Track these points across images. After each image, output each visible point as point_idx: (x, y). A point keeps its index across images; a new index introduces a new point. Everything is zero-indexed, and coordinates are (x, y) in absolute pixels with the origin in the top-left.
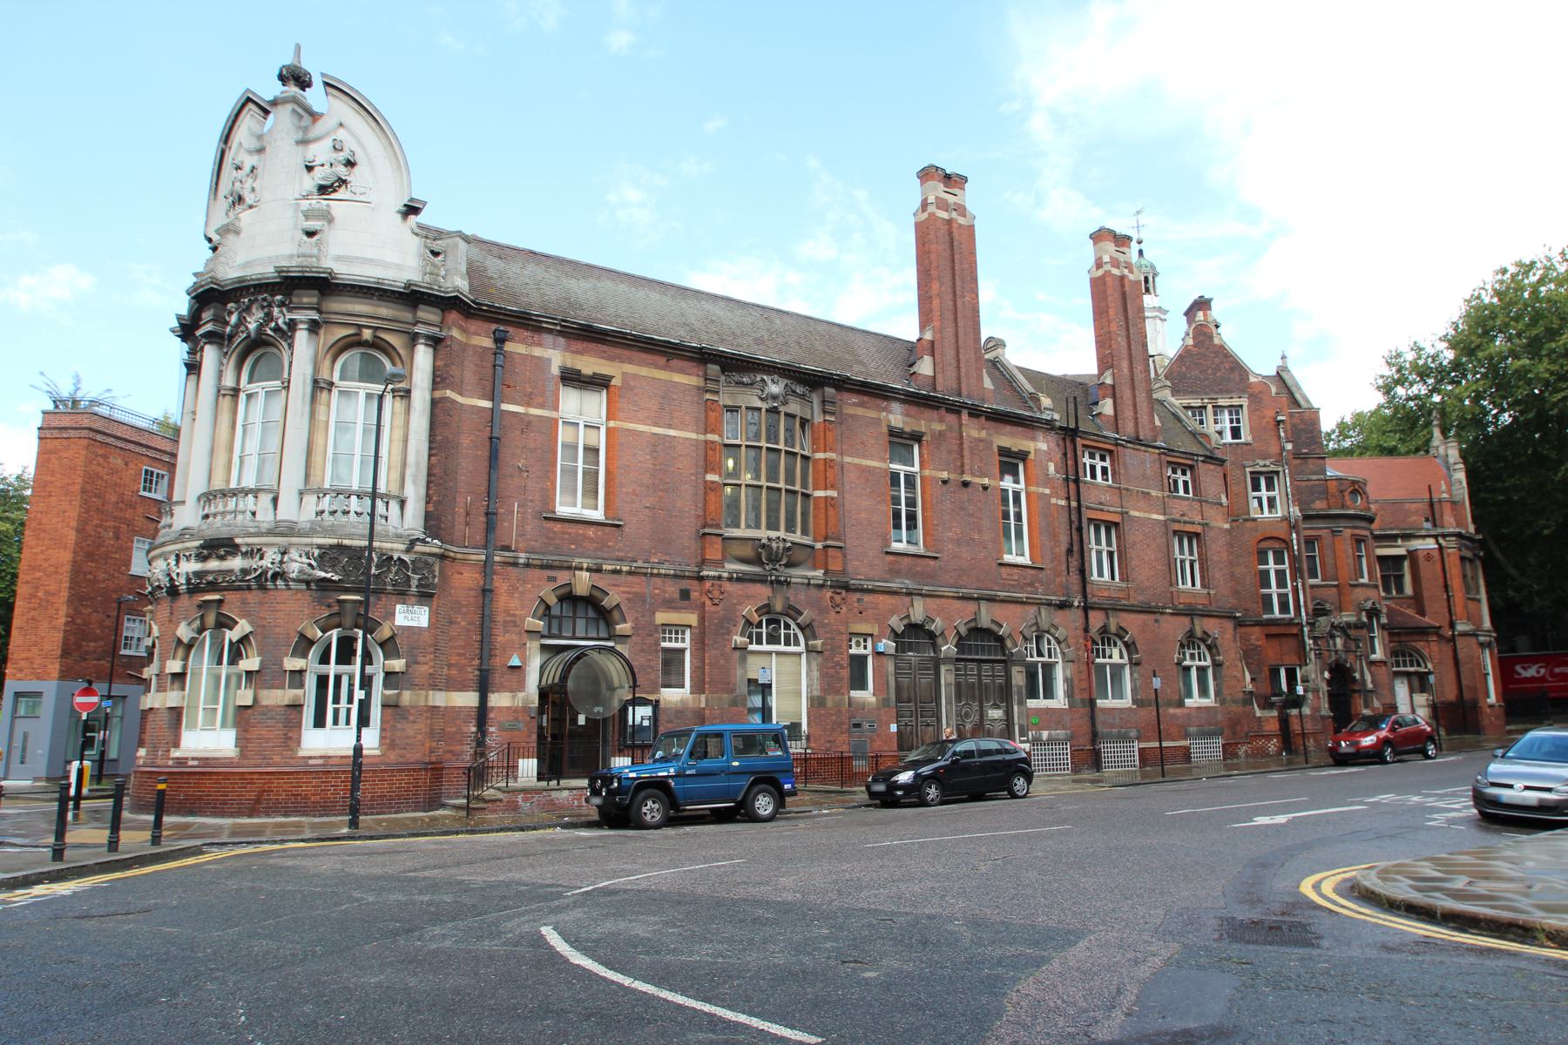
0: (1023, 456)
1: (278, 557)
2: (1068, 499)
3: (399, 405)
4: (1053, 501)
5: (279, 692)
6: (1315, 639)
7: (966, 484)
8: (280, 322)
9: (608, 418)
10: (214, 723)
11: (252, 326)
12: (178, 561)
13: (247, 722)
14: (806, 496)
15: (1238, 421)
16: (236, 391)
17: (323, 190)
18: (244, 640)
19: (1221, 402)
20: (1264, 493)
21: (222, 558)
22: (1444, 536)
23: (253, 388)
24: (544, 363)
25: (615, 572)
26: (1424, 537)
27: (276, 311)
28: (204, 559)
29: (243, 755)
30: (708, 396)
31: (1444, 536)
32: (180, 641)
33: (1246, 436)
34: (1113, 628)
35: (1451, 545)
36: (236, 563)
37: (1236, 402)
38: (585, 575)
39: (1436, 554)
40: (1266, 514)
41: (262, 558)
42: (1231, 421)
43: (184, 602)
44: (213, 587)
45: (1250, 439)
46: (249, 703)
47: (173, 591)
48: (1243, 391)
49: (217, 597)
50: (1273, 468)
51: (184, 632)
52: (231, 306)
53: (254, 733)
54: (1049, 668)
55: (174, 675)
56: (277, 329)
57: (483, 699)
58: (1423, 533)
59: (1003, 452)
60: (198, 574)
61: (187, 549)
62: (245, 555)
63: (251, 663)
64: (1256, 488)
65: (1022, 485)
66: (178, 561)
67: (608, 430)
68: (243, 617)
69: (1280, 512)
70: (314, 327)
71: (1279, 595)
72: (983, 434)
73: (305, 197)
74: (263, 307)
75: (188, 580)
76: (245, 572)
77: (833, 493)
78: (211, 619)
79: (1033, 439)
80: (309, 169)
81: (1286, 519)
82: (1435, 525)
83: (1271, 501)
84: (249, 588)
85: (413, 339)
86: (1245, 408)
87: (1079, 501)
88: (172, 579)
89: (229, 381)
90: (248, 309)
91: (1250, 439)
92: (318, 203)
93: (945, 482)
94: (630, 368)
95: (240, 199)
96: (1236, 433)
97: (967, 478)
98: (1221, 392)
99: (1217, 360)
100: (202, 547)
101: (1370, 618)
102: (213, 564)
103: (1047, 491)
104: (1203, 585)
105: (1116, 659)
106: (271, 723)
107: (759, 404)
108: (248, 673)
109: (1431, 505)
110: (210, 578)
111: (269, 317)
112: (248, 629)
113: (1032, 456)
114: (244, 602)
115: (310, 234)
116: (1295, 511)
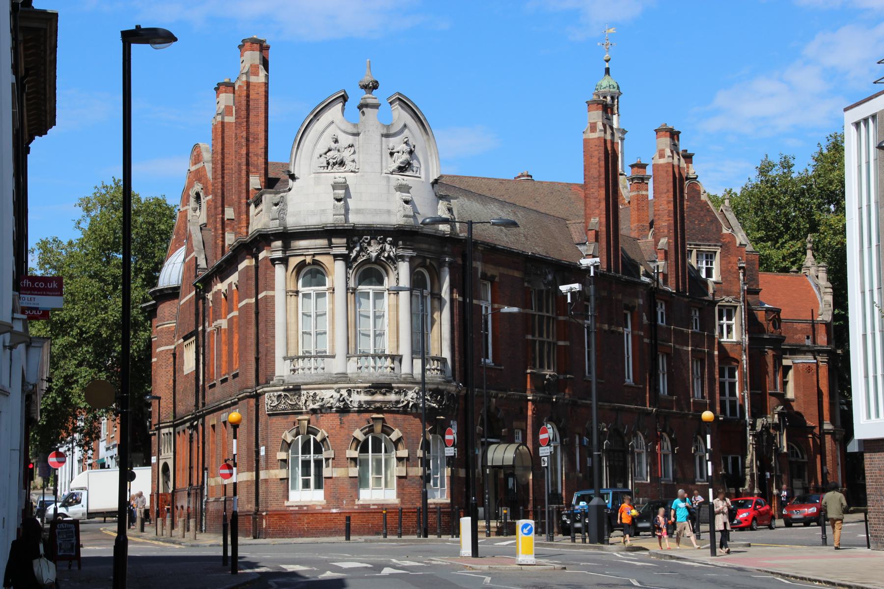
0: (631, 309)
1: (415, 396)
2: (651, 338)
3: (436, 303)
4: (646, 340)
5: (416, 469)
6: (754, 436)
7: (613, 332)
8: (391, 254)
9: (493, 302)
10: (380, 485)
11: (374, 254)
12: (349, 395)
13: (403, 485)
14: (554, 344)
15: (711, 264)
16: (354, 290)
17: (401, 169)
18: (399, 440)
19: (703, 248)
20: (725, 321)
21: (384, 394)
22: (820, 352)
23: (363, 288)
24: (476, 269)
25: (502, 397)
26: (804, 352)
27: (388, 247)
28: (373, 394)
29: (402, 502)
30: (526, 284)
31: (820, 352)
32: (355, 438)
33: (716, 277)
34: (668, 429)
35: (822, 359)
36: (392, 397)
37: (712, 249)
38: (494, 400)
39: (814, 367)
40: (725, 339)
41: (405, 395)
42: (707, 264)
43: (353, 417)
44: (378, 410)
45: (720, 279)
46: (404, 474)
47: (344, 410)
48: (718, 241)
49: (381, 416)
50: (734, 304)
51: (359, 434)
52: (356, 239)
53: (408, 490)
54: (639, 454)
55: (352, 459)
56: (389, 257)
57: (467, 473)
58: (805, 348)
59: (627, 307)
60: (367, 402)
61: (358, 387)
62: (396, 393)
63: (403, 453)
64: (721, 318)
65: (630, 329)
66: (349, 395)
67: (493, 309)
68: (396, 427)
69: (735, 337)
70: (411, 259)
71: (730, 401)
72: (620, 297)
73: (391, 173)
74: (379, 243)
75: (360, 405)
76: (398, 402)
77: (567, 343)
78: (378, 428)
79: (637, 297)
80: (392, 154)
81: (738, 343)
82: (814, 342)
83: (729, 328)
84: (398, 412)
85: (441, 264)
86: (718, 255)
87: (656, 340)
88: (346, 403)
89: (352, 284)
90: (369, 244)
91: (720, 279)
92: (399, 179)
93: (605, 331)
94: (502, 270)
95: (342, 163)
96: (709, 273)
97: (613, 328)
98: (703, 240)
99: (702, 213)
100: (370, 387)
101: (779, 420)
102: (379, 397)
103: (642, 334)
104: (703, 397)
105: (665, 451)
106: (414, 485)
107: (543, 287)
108: (400, 459)
109: (813, 326)
110: (378, 405)
111: (383, 250)
112: (401, 435)
113: (636, 309)
114: (395, 419)
115: (407, 202)
116: (746, 338)
